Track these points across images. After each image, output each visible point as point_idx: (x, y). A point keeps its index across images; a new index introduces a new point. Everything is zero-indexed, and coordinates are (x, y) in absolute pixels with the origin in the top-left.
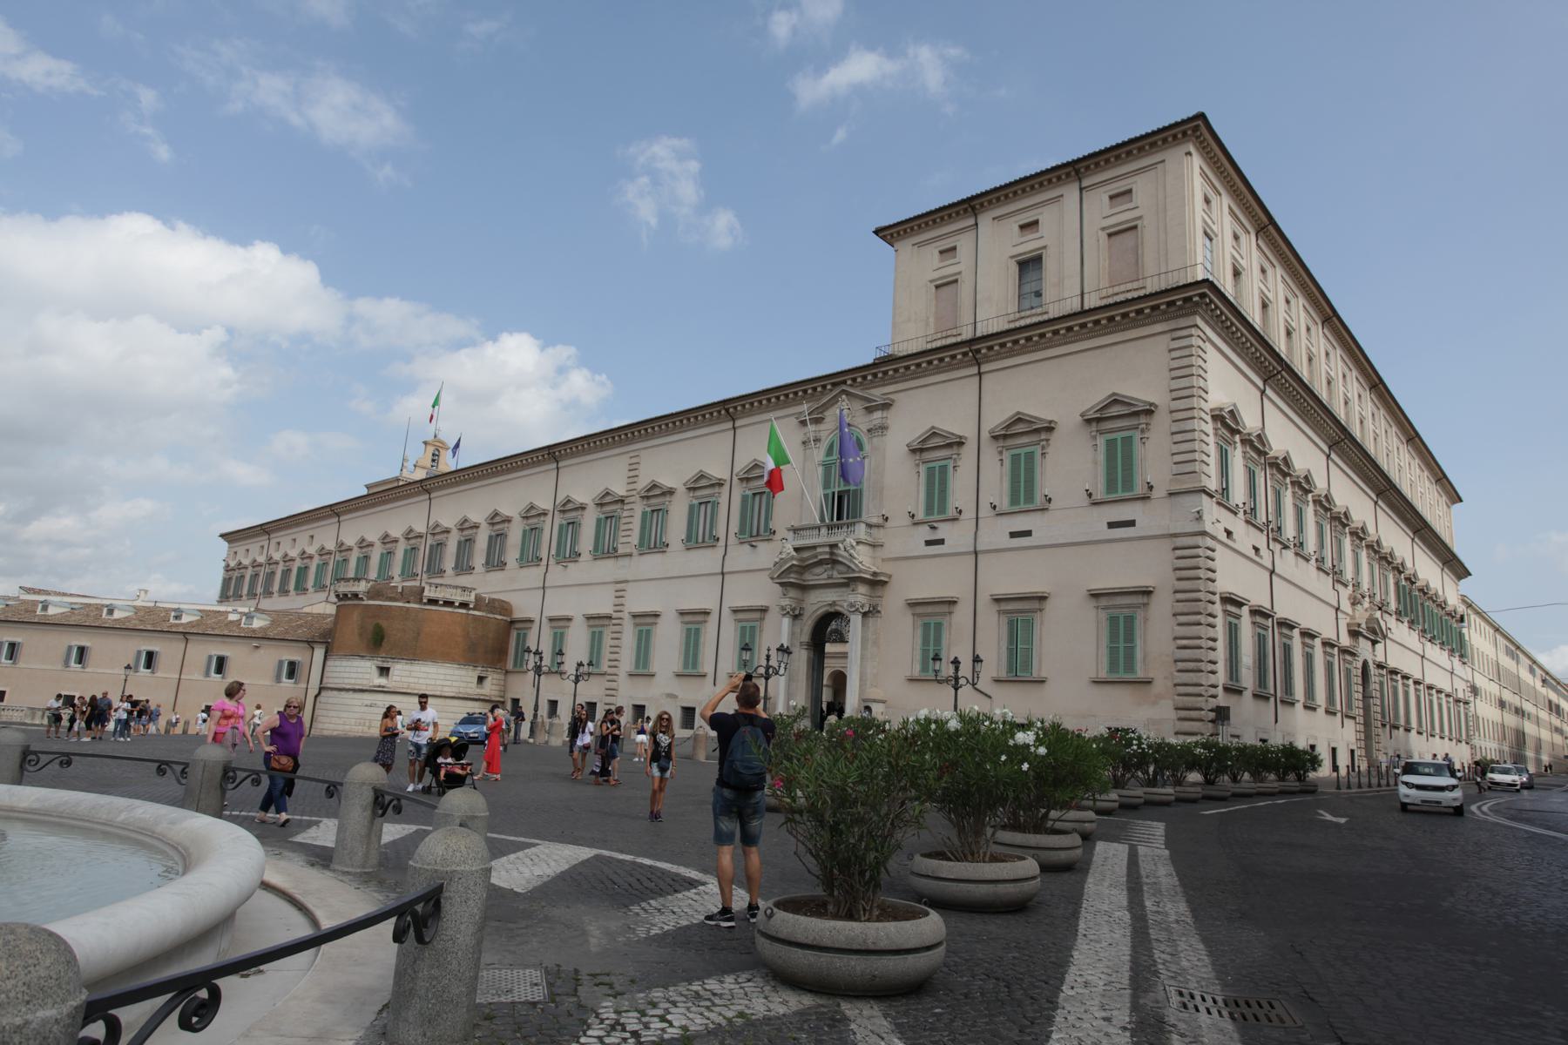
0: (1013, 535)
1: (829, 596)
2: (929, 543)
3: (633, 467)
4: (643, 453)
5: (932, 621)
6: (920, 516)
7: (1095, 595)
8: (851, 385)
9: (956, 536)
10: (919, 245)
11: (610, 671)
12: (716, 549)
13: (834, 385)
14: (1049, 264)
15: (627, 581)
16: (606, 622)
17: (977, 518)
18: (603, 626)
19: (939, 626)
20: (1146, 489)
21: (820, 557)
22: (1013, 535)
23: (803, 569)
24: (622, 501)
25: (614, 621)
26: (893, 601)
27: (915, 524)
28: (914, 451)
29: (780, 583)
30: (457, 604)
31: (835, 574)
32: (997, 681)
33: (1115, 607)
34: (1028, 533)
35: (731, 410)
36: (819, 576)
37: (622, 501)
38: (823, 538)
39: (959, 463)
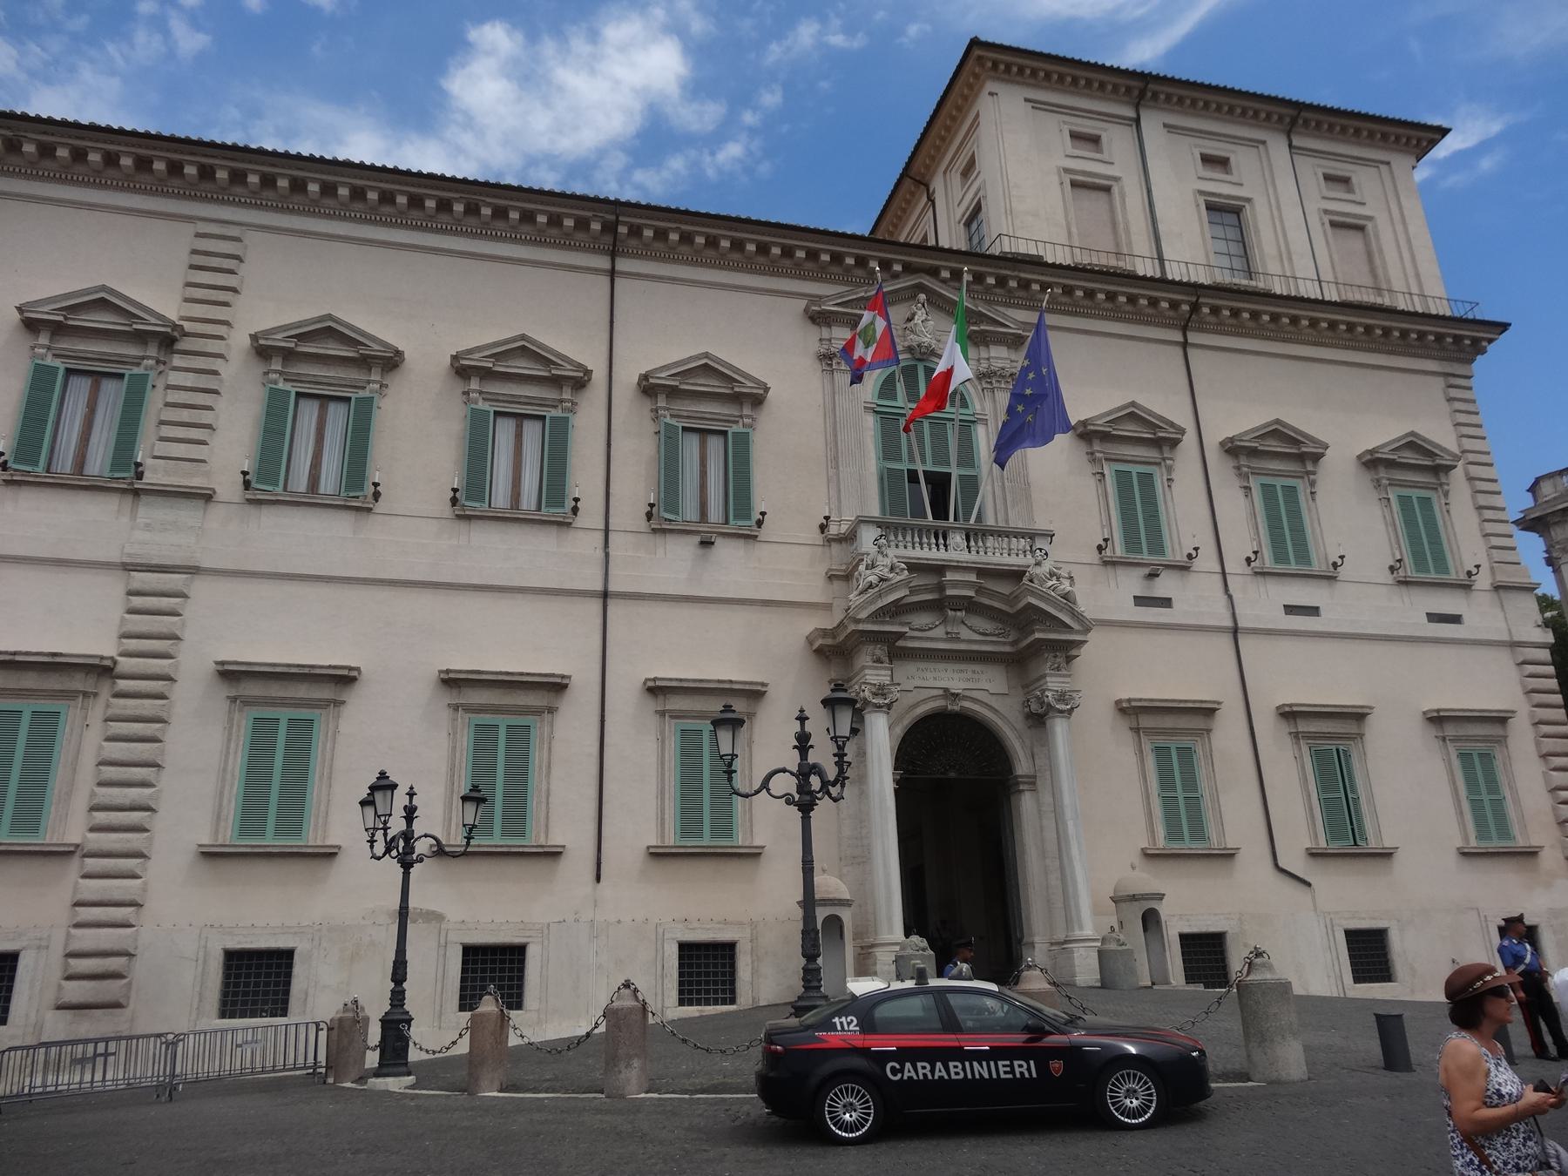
0: (1290, 609)
1: (954, 679)
2: (1140, 601)
4: (252, 237)
5: (1174, 743)
6: (1118, 549)
7: (1437, 719)
8: (944, 281)
10: (1036, 105)
12: (570, 535)
13: (909, 269)
15: (193, 570)
16: (78, 682)
17: (1224, 573)
18: (69, 695)
19: (1186, 754)
20: (1463, 576)
21: (949, 592)
22: (1290, 609)
23: (897, 610)
24: (168, 340)
25: (123, 684)
27: (1106, 563)
31: (965, 633)
32: (1314, 854)
33: (1468, 739)
34: (1313, 611)
35: (623, 230)
36: (927, 631)
38: (957, 551)
39: (1173, 476)
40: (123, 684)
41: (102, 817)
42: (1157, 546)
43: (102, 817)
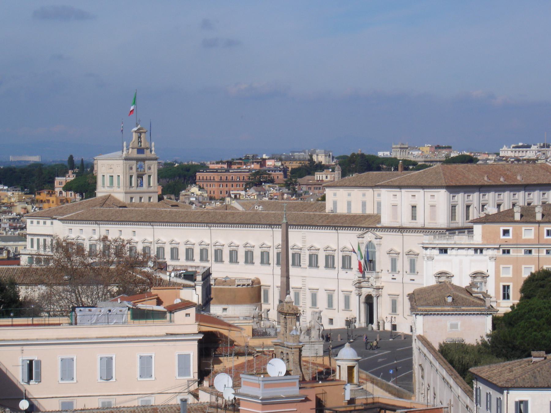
0: (411, 280)
2: (393, 279)
3: (304, 238)
6: (390, 271)
9: (398, 277)
11: (303, 306)
13: (366, 229)
14: (417, 208)
15: (306, 277)
22: (411, 280)
23: (360, 283)
26: (384, 293)
28: (388, 254)
29: (356, 287)
30: (246, 285)
37: (301, 249)
40: (303, 290)
41: (303, 303)
42: (395, 271)
43: (303, 303)
